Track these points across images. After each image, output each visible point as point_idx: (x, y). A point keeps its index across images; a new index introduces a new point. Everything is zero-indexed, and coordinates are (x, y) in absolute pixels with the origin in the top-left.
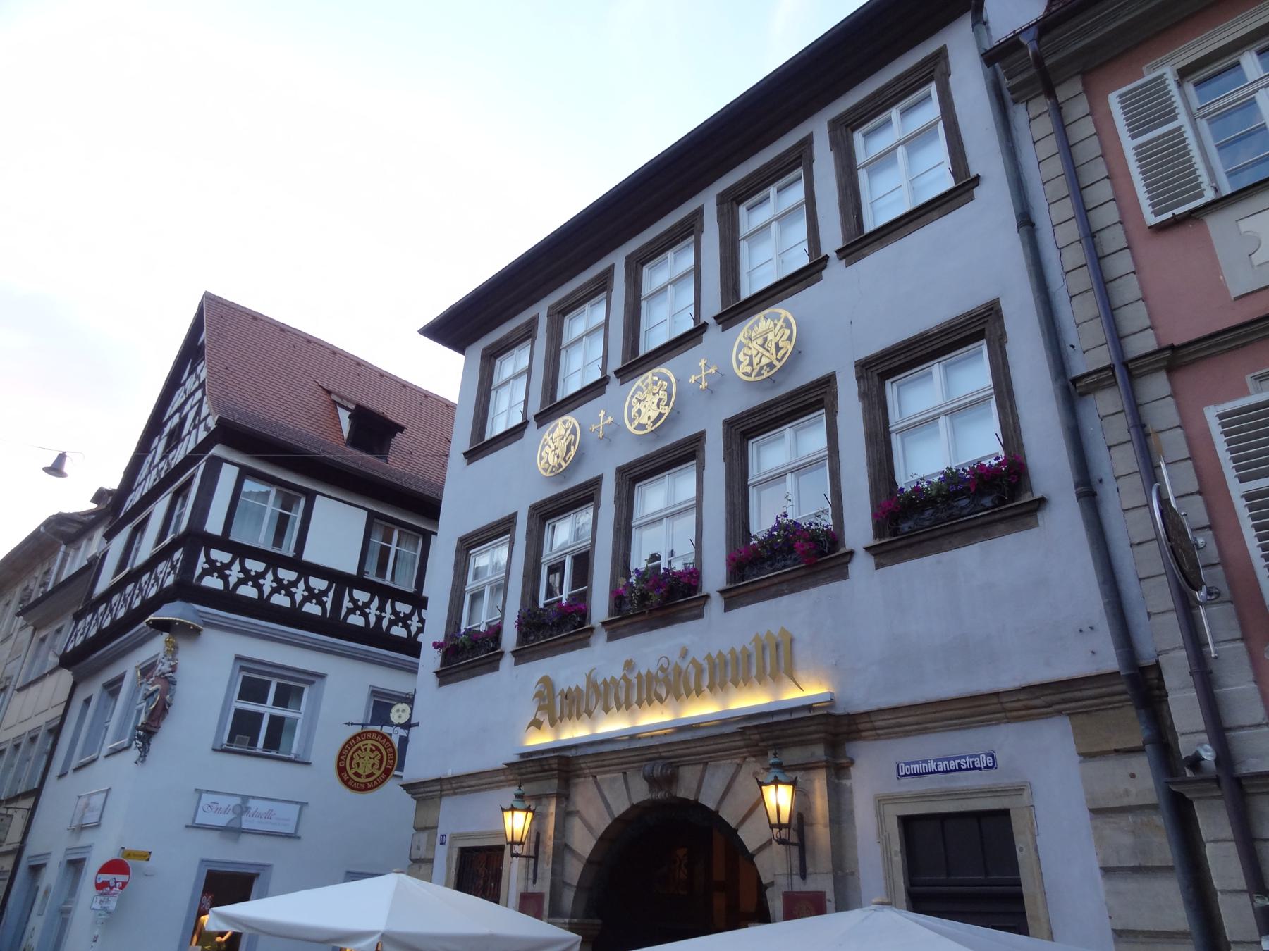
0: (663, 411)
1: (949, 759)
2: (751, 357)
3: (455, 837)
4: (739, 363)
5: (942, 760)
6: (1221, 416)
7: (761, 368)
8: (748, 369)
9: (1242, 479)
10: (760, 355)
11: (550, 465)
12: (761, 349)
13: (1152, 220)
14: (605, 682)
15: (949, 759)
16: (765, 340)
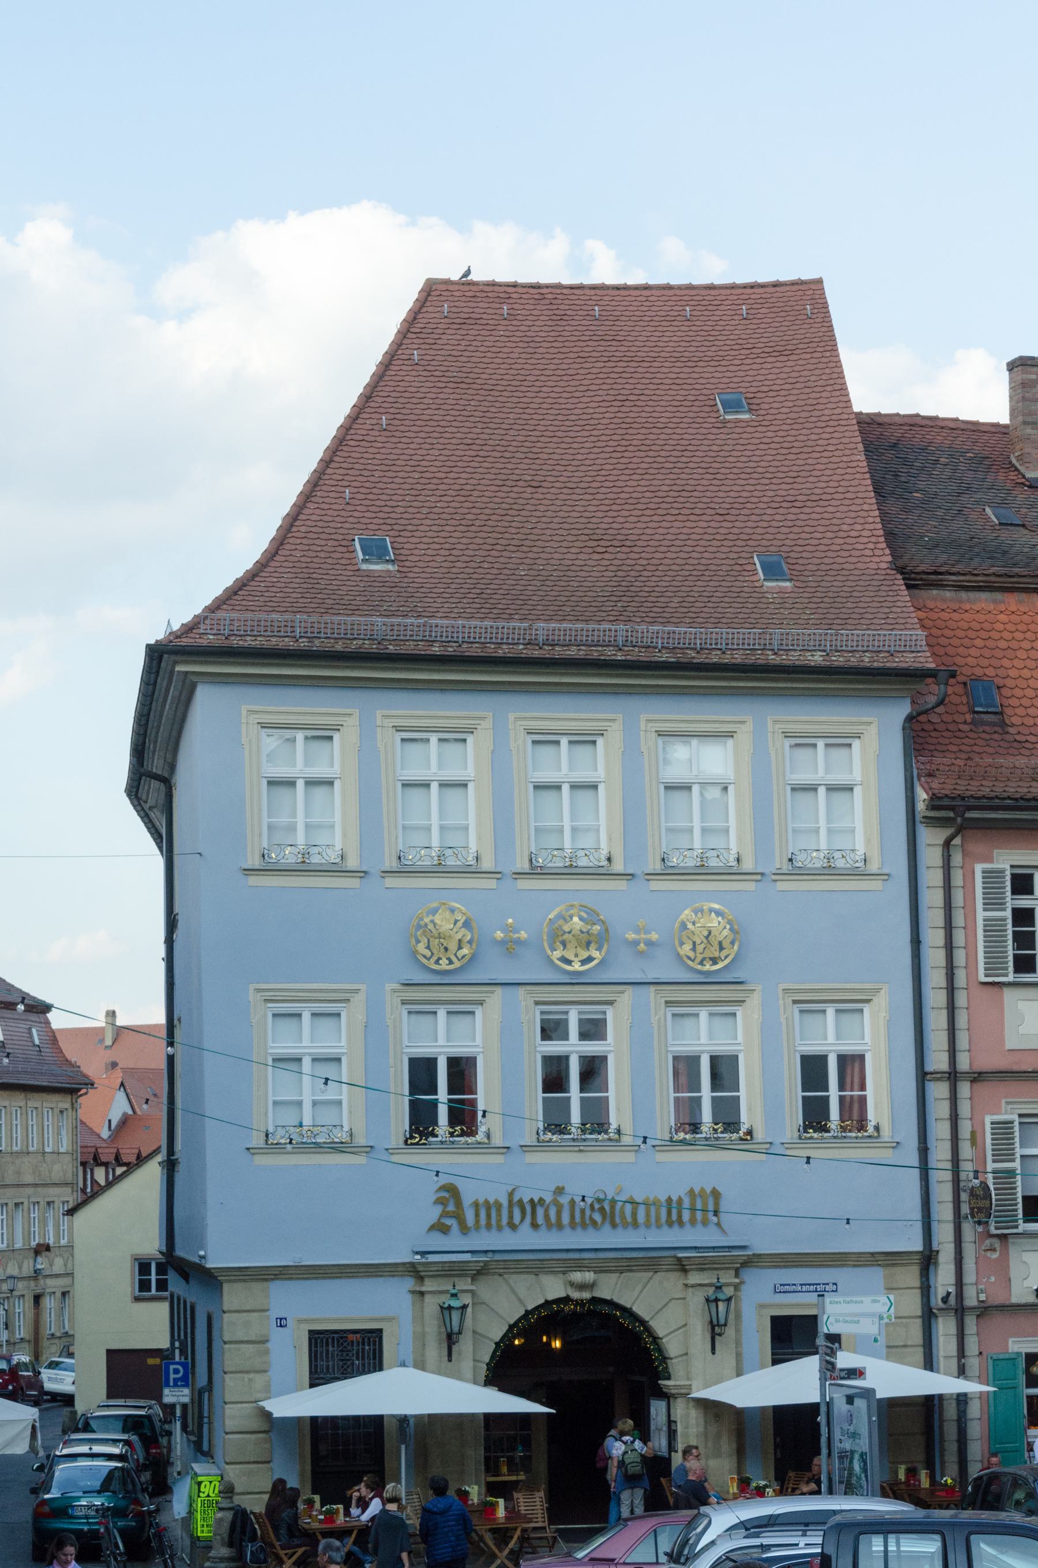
0: (594, 956)
1: (810, 1285)
2: (694, 943)
3: (300, 1321)
4: (682, 944)
5: (805, 1285)
6: (992, 1123)
7: (704, 959)
8: (691, 954)
9: (994, 1161)
10: (703, 946)
11: (433, 954)
12: (705, 941)
13: (983, 979)
14: (532, 1201)
15: (810, 1285)
16: (710, 933)
